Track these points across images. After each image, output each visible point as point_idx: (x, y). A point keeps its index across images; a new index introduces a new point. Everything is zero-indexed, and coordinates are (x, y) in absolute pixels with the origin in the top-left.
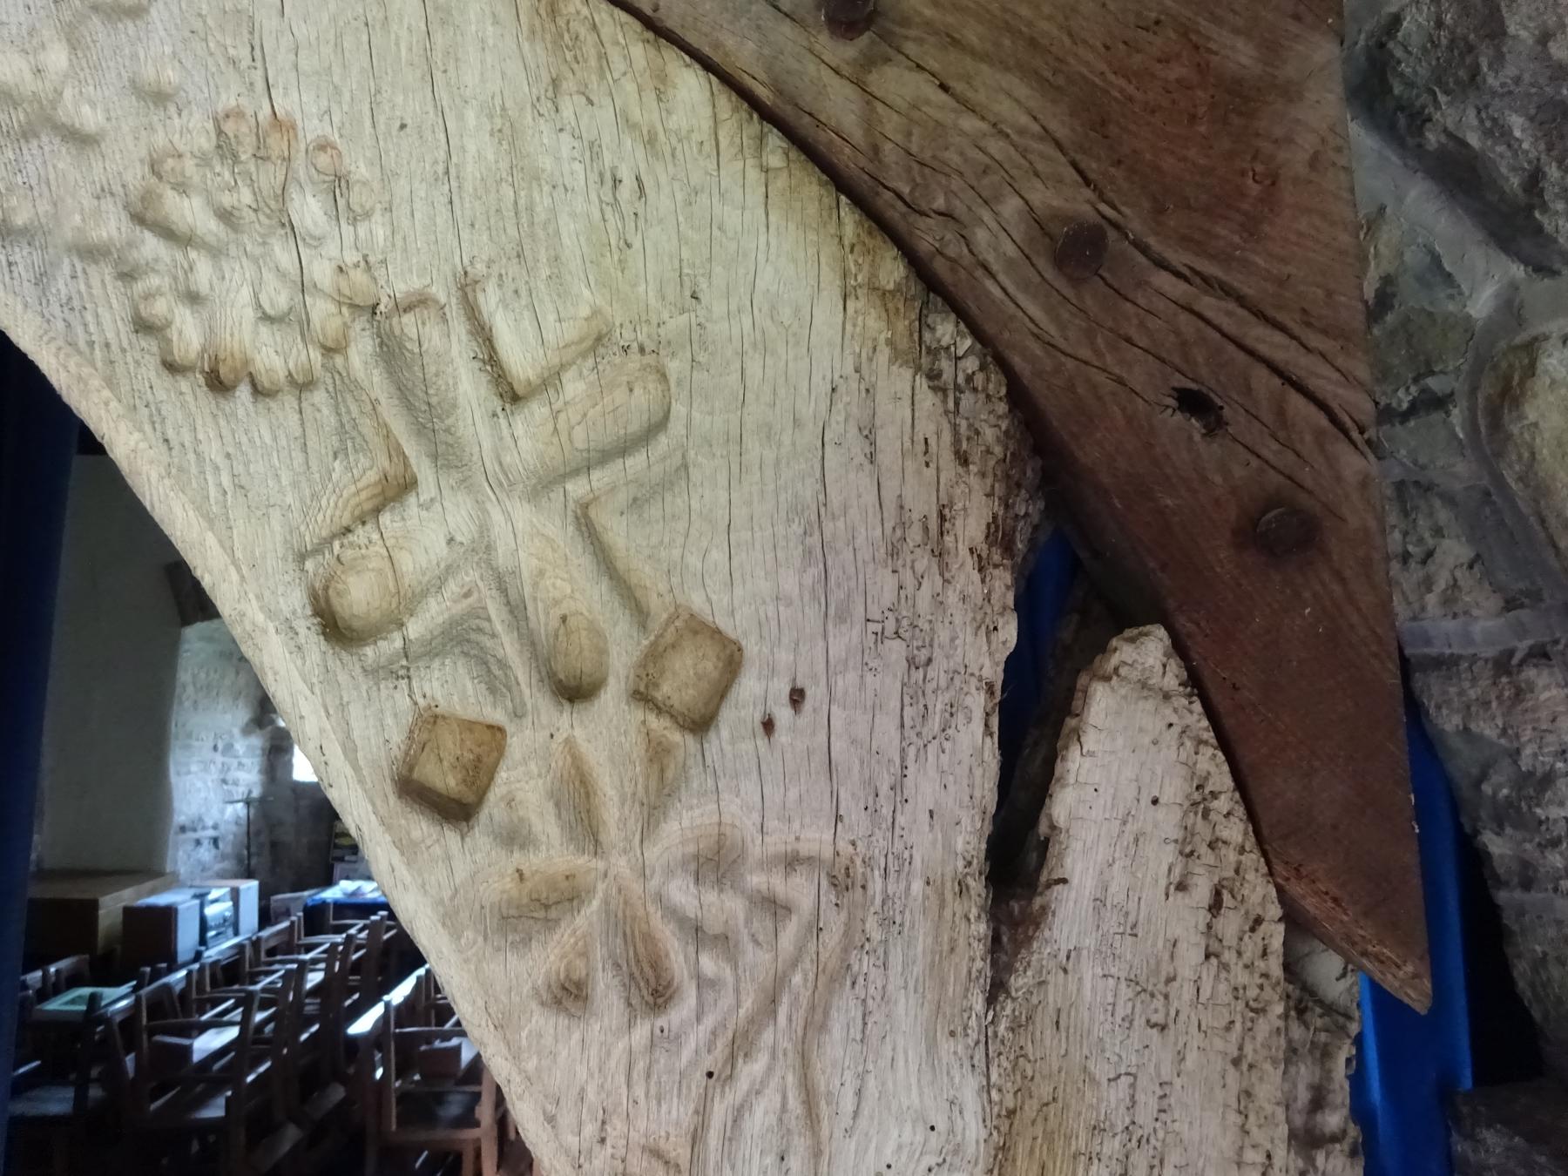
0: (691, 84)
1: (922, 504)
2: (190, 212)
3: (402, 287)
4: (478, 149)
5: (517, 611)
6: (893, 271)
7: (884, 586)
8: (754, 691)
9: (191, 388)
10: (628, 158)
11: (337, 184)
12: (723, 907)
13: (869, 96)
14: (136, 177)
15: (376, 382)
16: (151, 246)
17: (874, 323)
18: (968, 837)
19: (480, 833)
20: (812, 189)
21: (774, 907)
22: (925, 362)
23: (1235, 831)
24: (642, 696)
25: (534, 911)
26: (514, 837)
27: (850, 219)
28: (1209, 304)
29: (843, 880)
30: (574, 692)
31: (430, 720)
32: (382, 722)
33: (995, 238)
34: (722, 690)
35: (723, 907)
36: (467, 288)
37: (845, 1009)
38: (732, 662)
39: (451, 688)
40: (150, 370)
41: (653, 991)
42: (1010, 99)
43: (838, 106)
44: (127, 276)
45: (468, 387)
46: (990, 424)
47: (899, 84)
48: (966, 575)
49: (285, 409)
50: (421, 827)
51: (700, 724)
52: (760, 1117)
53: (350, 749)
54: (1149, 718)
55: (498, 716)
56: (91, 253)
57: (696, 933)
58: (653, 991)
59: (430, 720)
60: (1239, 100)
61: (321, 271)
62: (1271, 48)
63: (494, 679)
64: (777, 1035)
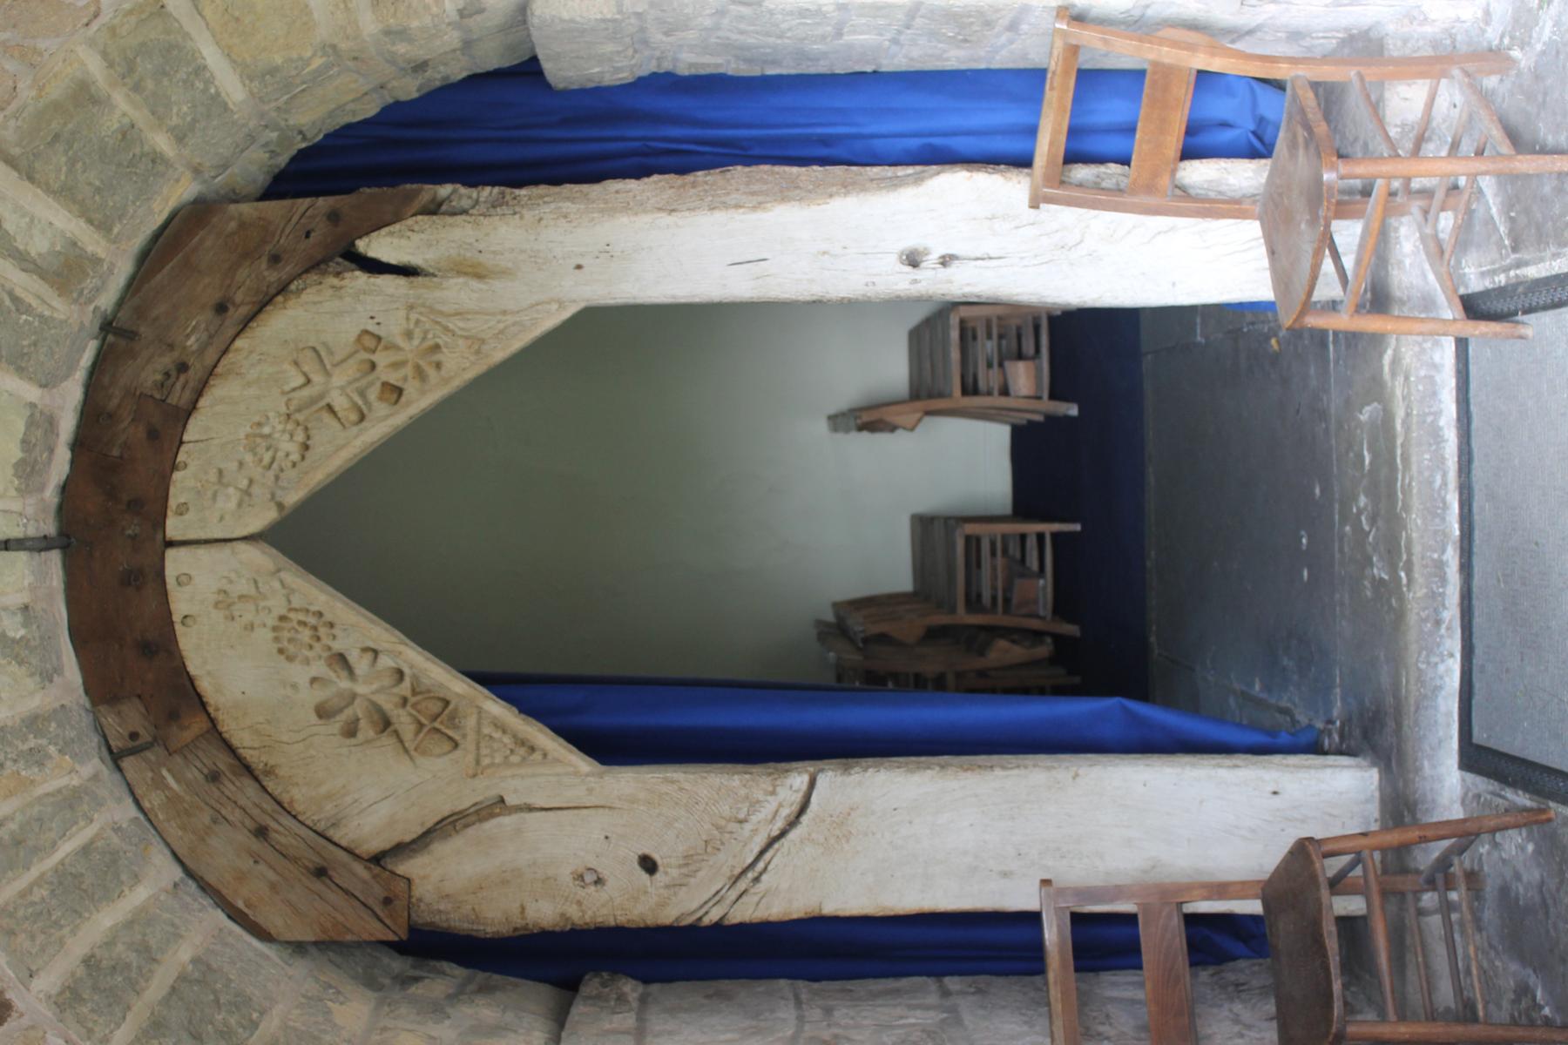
0: (239, 343)
1: (330, 292)
2: (267, 457)
3: (283, 409)
4: (253, 391)
5: (356, 380)
6: (280, 298)
7: (348, 299)
8: (371, 327)
9: (308, 454)
10: (255, 357)
11: (259, 424)
12: (418, 333)
13: (242, 303)
14: (260, 470)
15: (306, 412)
16: (275, 466)
17: (291, 303)
18: (401, 281)
19: (405, 386)
20: (262, 316)
21: (418, 322)
22: (300, 291)
23: (397, 227)
24: (374, 352)
25: (420, 374)
26: (405, 379)
27: (269, 308)
28: (287, 231)
29: (411, 307)
30: (373, 366)
31: (381, 398)
32: (381, 409)
33: (273, 276)
34: (373, 335)
35: (418, 333)
36: (283, 393)
37: (438, 307)
38: (366, 332)
39: (373, 394)
40: (305, 464)
41: (437, 348)
42: (242, 274)
43: (244, 310)
44: (282, 470)
45: (306, 393)
46: (313, 277)
47: (239, 297)
48: (346, 282)
49: (312, 433)
50: (403, 399)
51: (379, 339)
52: (461, 324)
53: (387, 417)
54: (374, 244)
55: (378, 385)
56: (277, 478)
57: (424, 339)
58: (437, 348)
59: (381, 398)
60: (243, 225)
61: (280, 427)
62: (232, 218)
63: (371, 384)
64: (443, 321)
